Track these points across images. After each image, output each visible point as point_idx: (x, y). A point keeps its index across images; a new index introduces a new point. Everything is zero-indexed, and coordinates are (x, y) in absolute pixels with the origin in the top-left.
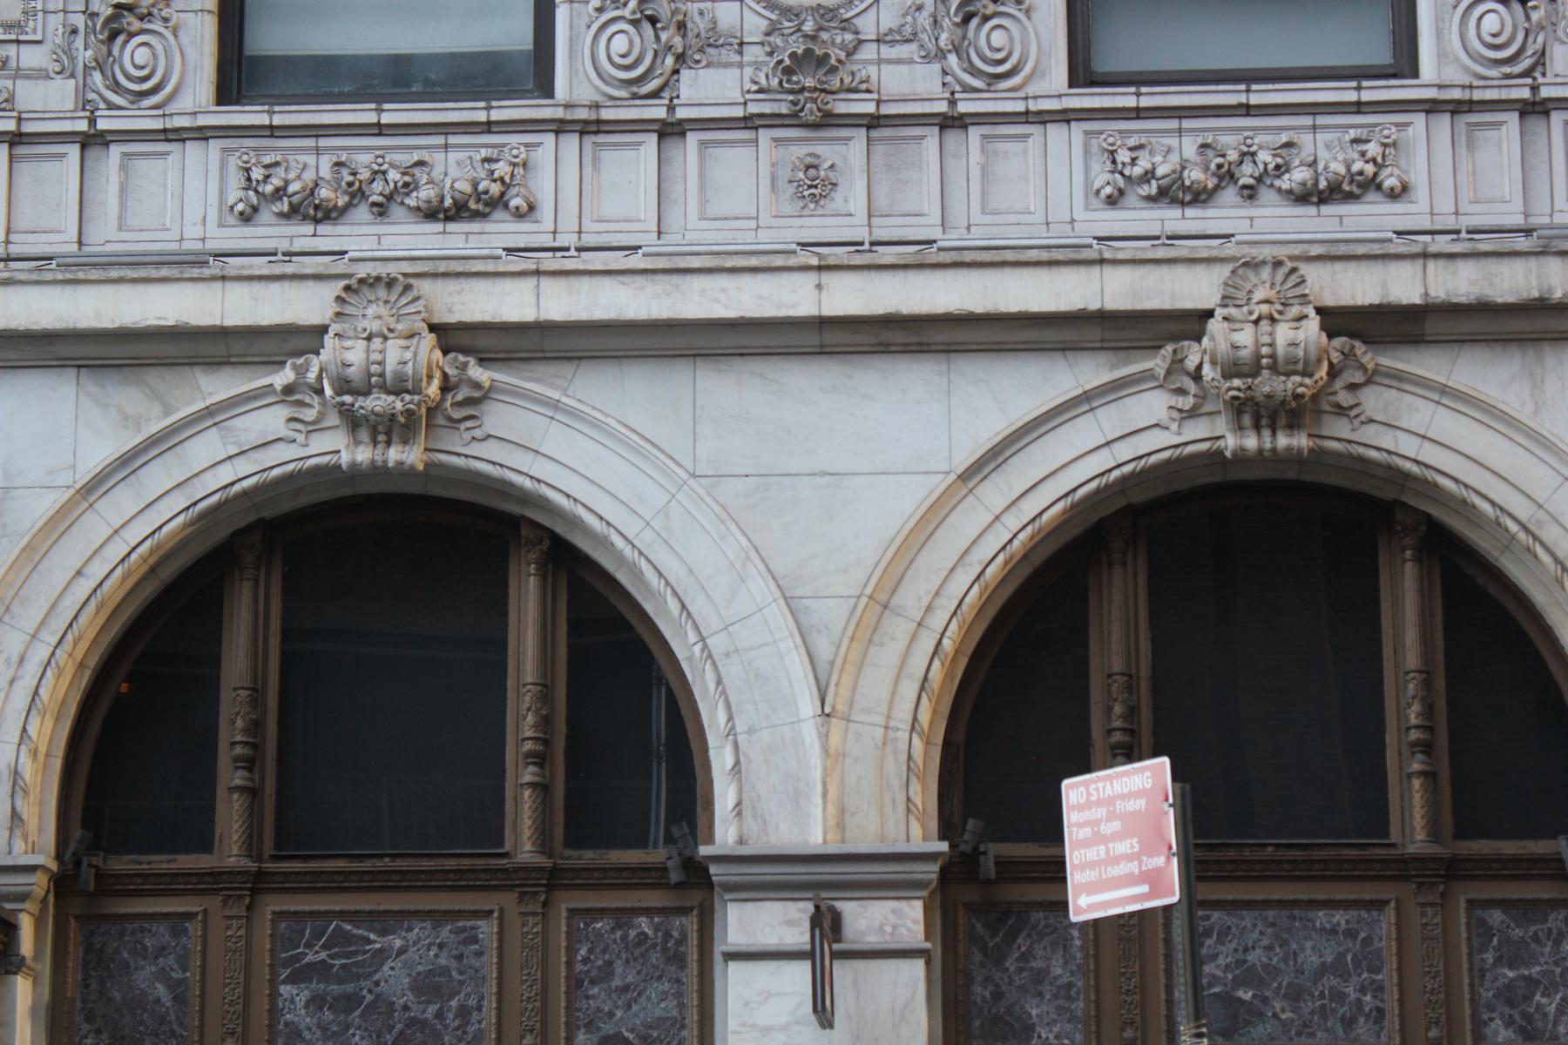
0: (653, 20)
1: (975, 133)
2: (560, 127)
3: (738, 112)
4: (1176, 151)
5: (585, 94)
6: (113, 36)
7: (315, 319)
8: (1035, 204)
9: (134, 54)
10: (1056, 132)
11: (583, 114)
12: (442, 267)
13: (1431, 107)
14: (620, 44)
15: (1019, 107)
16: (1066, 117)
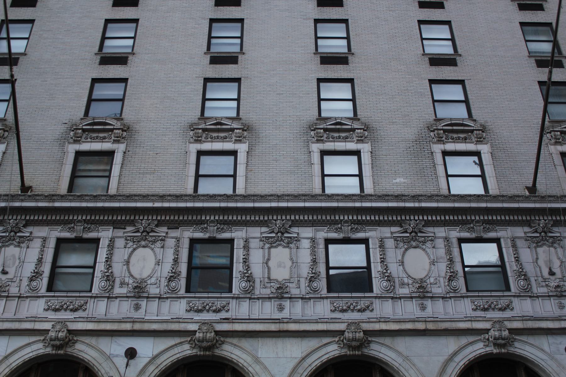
0: (389, 281)
1: (312, 300)
2: (233, 298)
3: (410, 296)
4: (481, 302)
5: (237, 293)
6: (310, 282)
7: (489, 328)
8: (464, 310)
9: (173, 284)
10: (325, 300)
11: (236, 296)
12: (452, 320)
13: (376, 297)
14: (244, 285)
15: (460, 295)
16: (327, 298)
